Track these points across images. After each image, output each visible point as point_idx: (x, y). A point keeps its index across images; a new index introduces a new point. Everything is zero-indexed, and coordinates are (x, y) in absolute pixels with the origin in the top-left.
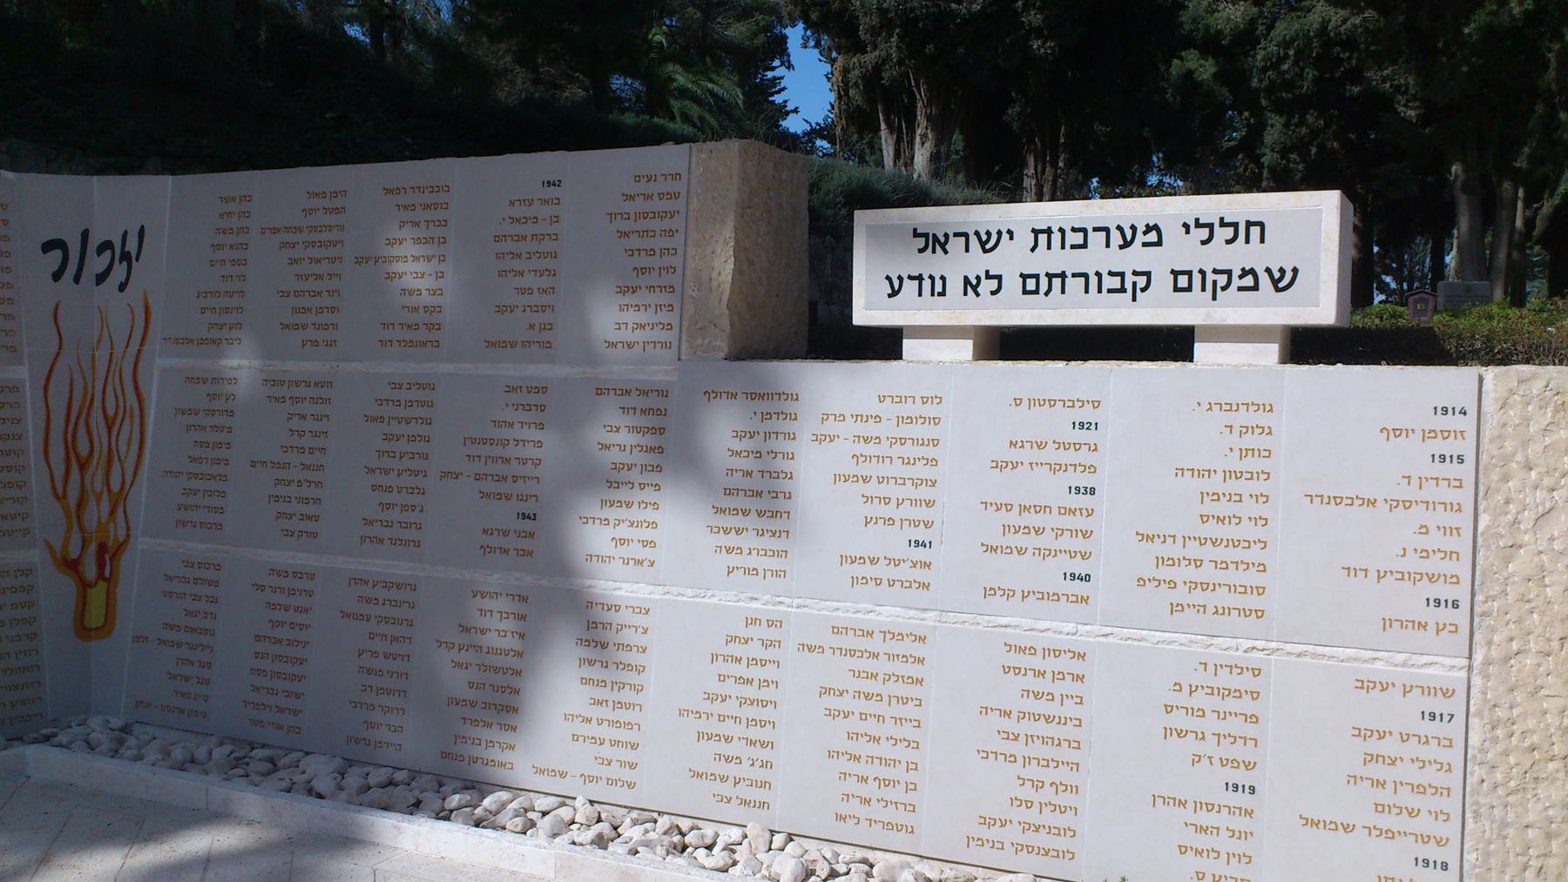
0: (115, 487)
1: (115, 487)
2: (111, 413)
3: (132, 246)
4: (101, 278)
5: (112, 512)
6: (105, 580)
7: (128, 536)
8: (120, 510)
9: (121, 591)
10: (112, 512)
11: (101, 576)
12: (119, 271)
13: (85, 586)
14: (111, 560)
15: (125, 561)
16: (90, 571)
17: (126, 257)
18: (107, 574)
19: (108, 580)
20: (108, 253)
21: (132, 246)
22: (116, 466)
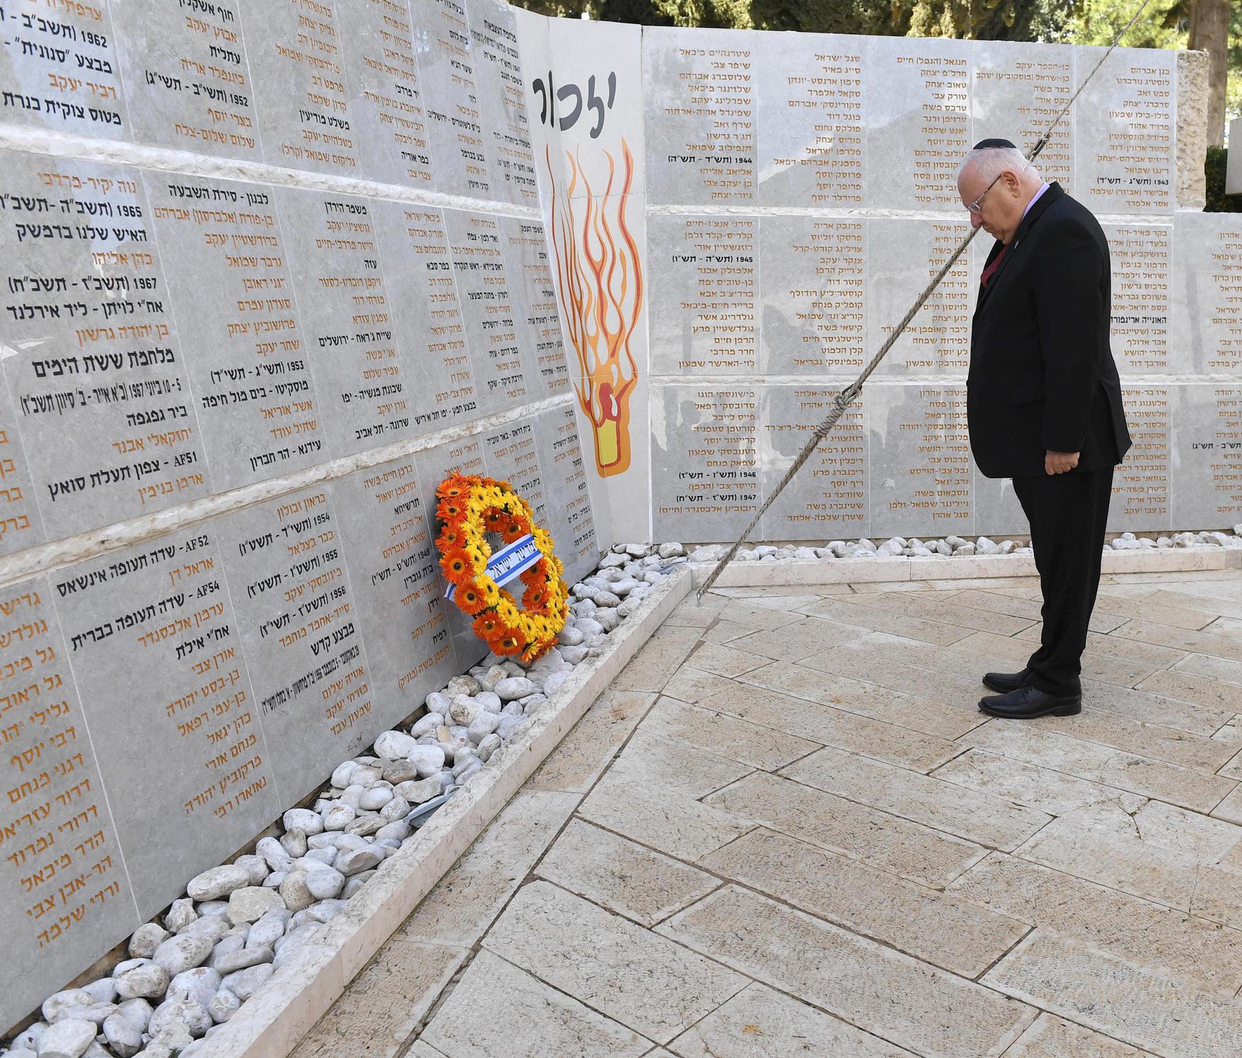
0: (613, 328)
1: (613, 328)
2: (597, 257)
3: (602, 91)
4: (567, 123)
5: (613, 354)
6: (612, 418)
7: (635, 376)
8: (622, 351)
9: (633, 428)
10: (613, 354)
11: (607, 414)
12: (589, 117)
13: (597, 425)
14: (618, 399)
15: (634, 399)
16: (598, 411)
17: (595, 102)
18: (615, 412)
19: (617, 419)
20: (573, 99)
21: (602, 91)
22: (611, 310)
